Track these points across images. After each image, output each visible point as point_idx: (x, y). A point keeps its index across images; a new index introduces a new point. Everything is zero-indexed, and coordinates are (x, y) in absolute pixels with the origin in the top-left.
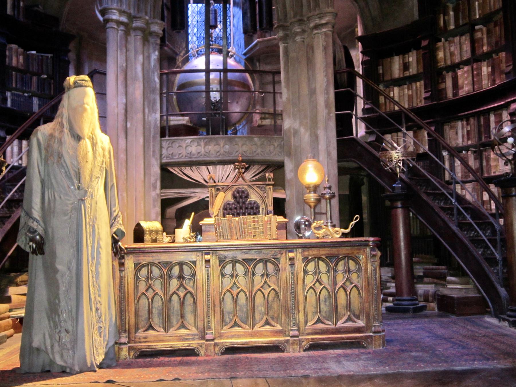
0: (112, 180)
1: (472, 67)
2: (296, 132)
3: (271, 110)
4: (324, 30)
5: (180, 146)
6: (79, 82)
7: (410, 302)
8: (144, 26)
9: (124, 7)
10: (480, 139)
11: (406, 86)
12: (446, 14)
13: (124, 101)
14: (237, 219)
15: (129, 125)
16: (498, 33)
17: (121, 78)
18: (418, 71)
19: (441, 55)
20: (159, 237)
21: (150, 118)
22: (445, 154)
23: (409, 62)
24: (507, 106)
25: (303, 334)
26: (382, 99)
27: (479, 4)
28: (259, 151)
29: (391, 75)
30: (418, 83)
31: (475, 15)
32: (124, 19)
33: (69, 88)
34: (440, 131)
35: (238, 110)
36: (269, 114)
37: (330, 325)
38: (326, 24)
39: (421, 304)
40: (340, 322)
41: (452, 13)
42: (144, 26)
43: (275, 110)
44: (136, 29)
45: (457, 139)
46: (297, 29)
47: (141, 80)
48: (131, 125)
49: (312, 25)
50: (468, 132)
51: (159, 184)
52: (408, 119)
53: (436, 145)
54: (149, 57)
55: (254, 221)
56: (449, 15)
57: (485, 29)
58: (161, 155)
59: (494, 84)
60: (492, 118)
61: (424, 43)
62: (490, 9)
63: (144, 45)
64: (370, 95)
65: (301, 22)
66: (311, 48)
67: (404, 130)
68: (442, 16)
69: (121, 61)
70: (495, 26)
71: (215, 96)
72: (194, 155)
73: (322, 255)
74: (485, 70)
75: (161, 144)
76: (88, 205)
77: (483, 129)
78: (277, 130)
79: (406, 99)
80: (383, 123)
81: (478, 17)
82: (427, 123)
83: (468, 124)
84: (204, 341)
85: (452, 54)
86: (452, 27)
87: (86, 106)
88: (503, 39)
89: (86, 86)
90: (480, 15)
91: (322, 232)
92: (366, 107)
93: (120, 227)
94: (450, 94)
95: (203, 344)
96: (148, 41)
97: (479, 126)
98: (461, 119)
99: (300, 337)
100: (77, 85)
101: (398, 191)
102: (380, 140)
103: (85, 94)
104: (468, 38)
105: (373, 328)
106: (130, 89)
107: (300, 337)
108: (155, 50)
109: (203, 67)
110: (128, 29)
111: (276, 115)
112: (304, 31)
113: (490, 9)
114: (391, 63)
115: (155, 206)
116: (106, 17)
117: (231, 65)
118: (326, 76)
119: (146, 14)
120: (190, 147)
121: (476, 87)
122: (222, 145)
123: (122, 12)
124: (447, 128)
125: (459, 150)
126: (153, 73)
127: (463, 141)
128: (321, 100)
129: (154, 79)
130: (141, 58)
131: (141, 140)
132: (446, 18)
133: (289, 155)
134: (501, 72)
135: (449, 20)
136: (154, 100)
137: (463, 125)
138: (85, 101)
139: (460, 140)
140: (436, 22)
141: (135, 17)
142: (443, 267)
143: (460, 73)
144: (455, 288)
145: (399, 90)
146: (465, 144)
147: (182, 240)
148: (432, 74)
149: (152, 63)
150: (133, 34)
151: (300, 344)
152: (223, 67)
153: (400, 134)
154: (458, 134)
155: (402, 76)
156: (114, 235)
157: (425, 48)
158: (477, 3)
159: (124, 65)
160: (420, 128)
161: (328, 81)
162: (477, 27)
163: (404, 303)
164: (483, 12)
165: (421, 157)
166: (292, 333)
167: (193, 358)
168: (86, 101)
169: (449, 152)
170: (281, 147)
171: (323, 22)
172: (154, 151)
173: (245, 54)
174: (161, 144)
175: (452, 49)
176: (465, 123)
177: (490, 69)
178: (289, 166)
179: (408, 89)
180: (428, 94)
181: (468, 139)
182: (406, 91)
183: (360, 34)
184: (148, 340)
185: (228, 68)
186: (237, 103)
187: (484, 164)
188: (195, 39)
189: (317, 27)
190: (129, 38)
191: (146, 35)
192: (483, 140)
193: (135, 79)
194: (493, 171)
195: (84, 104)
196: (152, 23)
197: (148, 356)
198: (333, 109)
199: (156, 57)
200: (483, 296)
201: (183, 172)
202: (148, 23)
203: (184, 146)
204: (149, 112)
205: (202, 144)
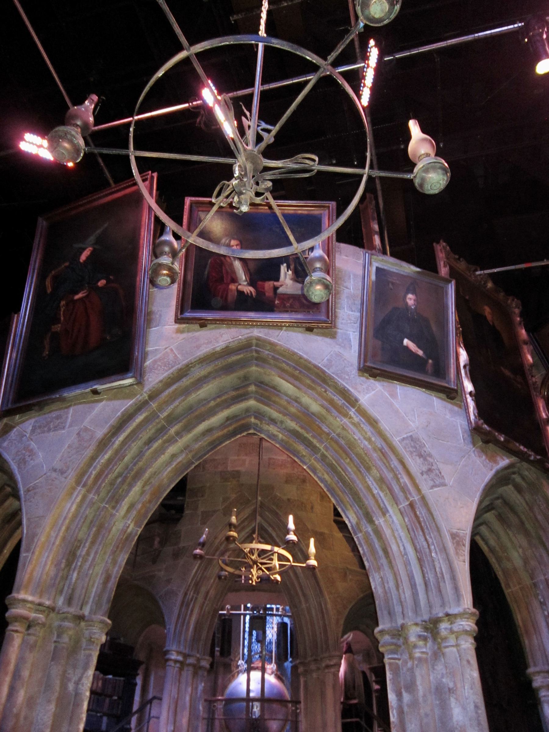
8: (195, 662)
9: (182, 649)
32: (180, 658)
42: (195, 662)
119: (198, 652)
123: (179, 653)
150: (186, 668)
190: (182, 673)
191: (197, 668)
202: (198, 660)
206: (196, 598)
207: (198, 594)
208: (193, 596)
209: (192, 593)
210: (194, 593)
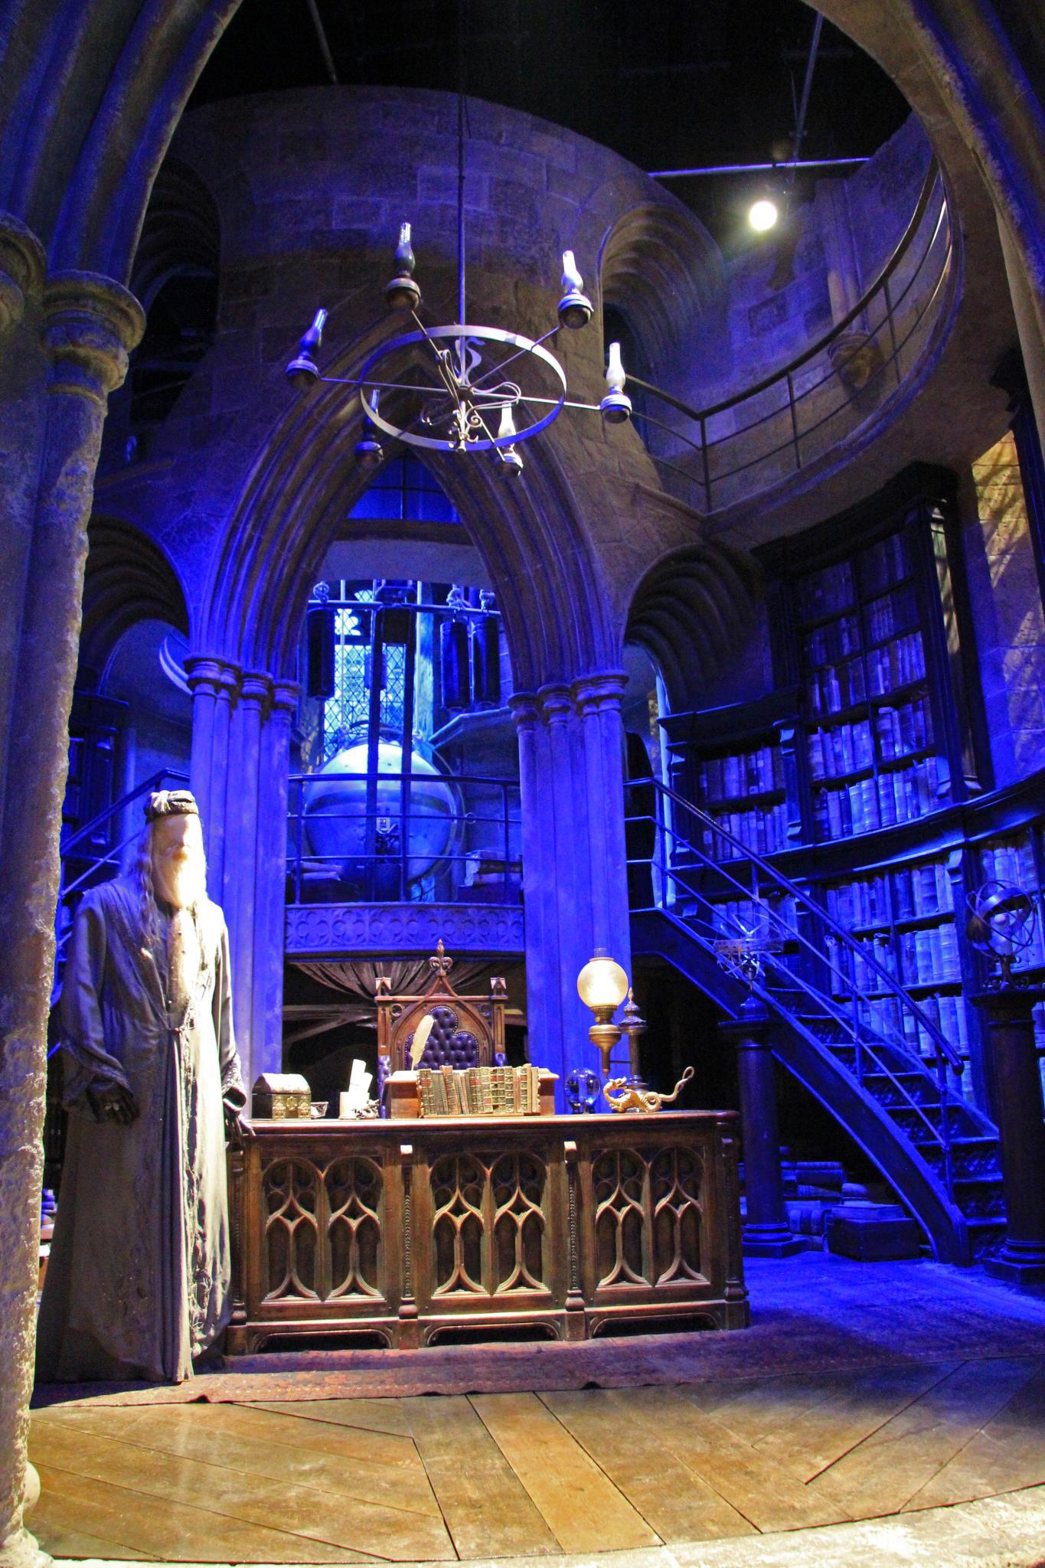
0: (224, 993)
1: (876, 783)
2: (550, 900)
3: (501, 854)
4: (603, 707)
5: (323, 922)
7: (775, 1236)
9: (230, 657)
10: (895, 916)
11: (753, 814)
12: (824, 683)
13: (221, 831)
14: (461, 1073)
15: (227, 880)
16: (921, 723)
17: (218, 788)
18: (774, 785)
19: (817, 757)
20: (303, 1106)
21: (267, 866)
22: (830, 943)
23: (757, 769)
24: (943, 856)
25: (591, 1304)
26: (708, 837)
27: (884, 669)
28: (476, 934)
29: (723, 791)
30: (776, 809)
31: (878, 688)
32: (227, 678)
34: (821, 899)
35: (425, 853)
36: (496, 862)
37: (644, 1284)
38: (609, 697)
39: (797, 1238)
40: (663, 1278)
41: (834, 683)
43: (507, 856)
44: (246, 697)
45: (852, 915)
46: (551, 704)
47: (254, 792)
48: (232, 879)
49: (581, 697)
50: (872, 902)
51: (279, 996)
52: (763, 876)
53: (814, 926)
54: (270, 748)
55: (494, 1079)
56: (829, 685)
57: (896, 714)
58: (286, 938)
59: (919, 815)
60: (916, 878)
61: (787, 735)
62: (905, 679)
63: (262, 726)
64: (685, 826)
65: (559, 691)
66: (578, 741)
67: (756, 897)
68: (817, 686)
69: (220, 754)
70: (915, 709)
71: (385, 825)
72: (349, 940)
73: (630, 1145)
74: (900, 788)
75: (286, 917)
76: (183, 1041)
77: (901, 897)
78: (514, 894)
79: (754, 837)
80: (711, 883)
81: (882, 692)
82: (797, 884)
83: (871, 888)
84: (397, 1318)
85: (838, 757)
86: (836, 708)
88: (931, 734)
89: (188, 812)
90: (886, 688)
91: (624, 1099)
92: (679, 850)
94: (835, 831)
95: (395, 1322)
96: (268, 719)
97: (894, 892)
98: (859, 877)
99: (587, 1310)
101: (748, 1018)
102: (706, 915)
103: (183, 827)
104: (867, 728)
105: (727, 1290)
106: (232, 809)
107: (587, 1310)
108: (281, 737)
109: (363, 769)
110: (235, 696)
111: (509, 865)
112: (565, 708)
113: (905, 679)
114: (722, 771)
115: (269, 1041)
116: (196, 673)
117: (418, 768)
118: (609, 792)
119: (268, 670)
120: (346, 922)
121: (884, 818)
122: (405, 920)
123: (225, 666)
124: (831, 893)
125: (860, 935)
126: (276, 778)
127: (864, 921)
128: (598, 839)
129: (277, 791)
130: (254, 751)
131: (250, 910)
132: (825, 689)
133: (537, 942)
134: (931, 794)
135: (830, 693)
136: (277, 830)
137: (862, 889)
139: (857, 919)
140: (804, 698)
141: (248, 675)
142: (836, 1164)
143: (853, 791)
144: (857, 1206)
145: (741, 820)
146: (867, 926)
147: (354, 1115)
148: (807, 792)
149: (275, 763)
150: (241, 705)
151: (587, 1324)
152: (403, 769)
153: (743, 904)
154: (853, 908)
155: (744, 794)
157: (787, 744)
158: (880, 667)
159: (224, 763)
160: (784, 892)
161: (613, 801)
162: (882, 710)
163: (765, 1237)
164: (892, 684)
165: (792, 946)
166: (569, 1301)
167: (376, 1353)
169: (839, 939)
170: (521, 925)
171: (603, 692)
172: (272, 932)
173: (434, 742)
174: (286, 917)
175: (838, 748)
176: (865, 885)
177: (909, 787)
178: (534, 965)
179: (758, 819)
180: (797, 830)
181: (874, 915)
182: (753, 823)
183: (661, 715)
184: (287, 1313)
185: (413, 772)
186: (425, 836)
187: (905, 963)
188: (336, 709)
189: (591, 701)
190: (234, 713)
192: (904, 919)
193: (243, 792)
194: (921, 976)
195: (182, 845)
196: (279, 686)
197: (284, 1347)
198: (624, 854)
199: (282, 750)
200: (916, 1221)
201: (326, 976)
202: (271, 688)
203: (331, 922)
204: (266, 854)
205: (367, 918)
206: (259, 540)
207: (264, 529)
208: (251, 538)
209: (249, 526)
210: (254, 527)
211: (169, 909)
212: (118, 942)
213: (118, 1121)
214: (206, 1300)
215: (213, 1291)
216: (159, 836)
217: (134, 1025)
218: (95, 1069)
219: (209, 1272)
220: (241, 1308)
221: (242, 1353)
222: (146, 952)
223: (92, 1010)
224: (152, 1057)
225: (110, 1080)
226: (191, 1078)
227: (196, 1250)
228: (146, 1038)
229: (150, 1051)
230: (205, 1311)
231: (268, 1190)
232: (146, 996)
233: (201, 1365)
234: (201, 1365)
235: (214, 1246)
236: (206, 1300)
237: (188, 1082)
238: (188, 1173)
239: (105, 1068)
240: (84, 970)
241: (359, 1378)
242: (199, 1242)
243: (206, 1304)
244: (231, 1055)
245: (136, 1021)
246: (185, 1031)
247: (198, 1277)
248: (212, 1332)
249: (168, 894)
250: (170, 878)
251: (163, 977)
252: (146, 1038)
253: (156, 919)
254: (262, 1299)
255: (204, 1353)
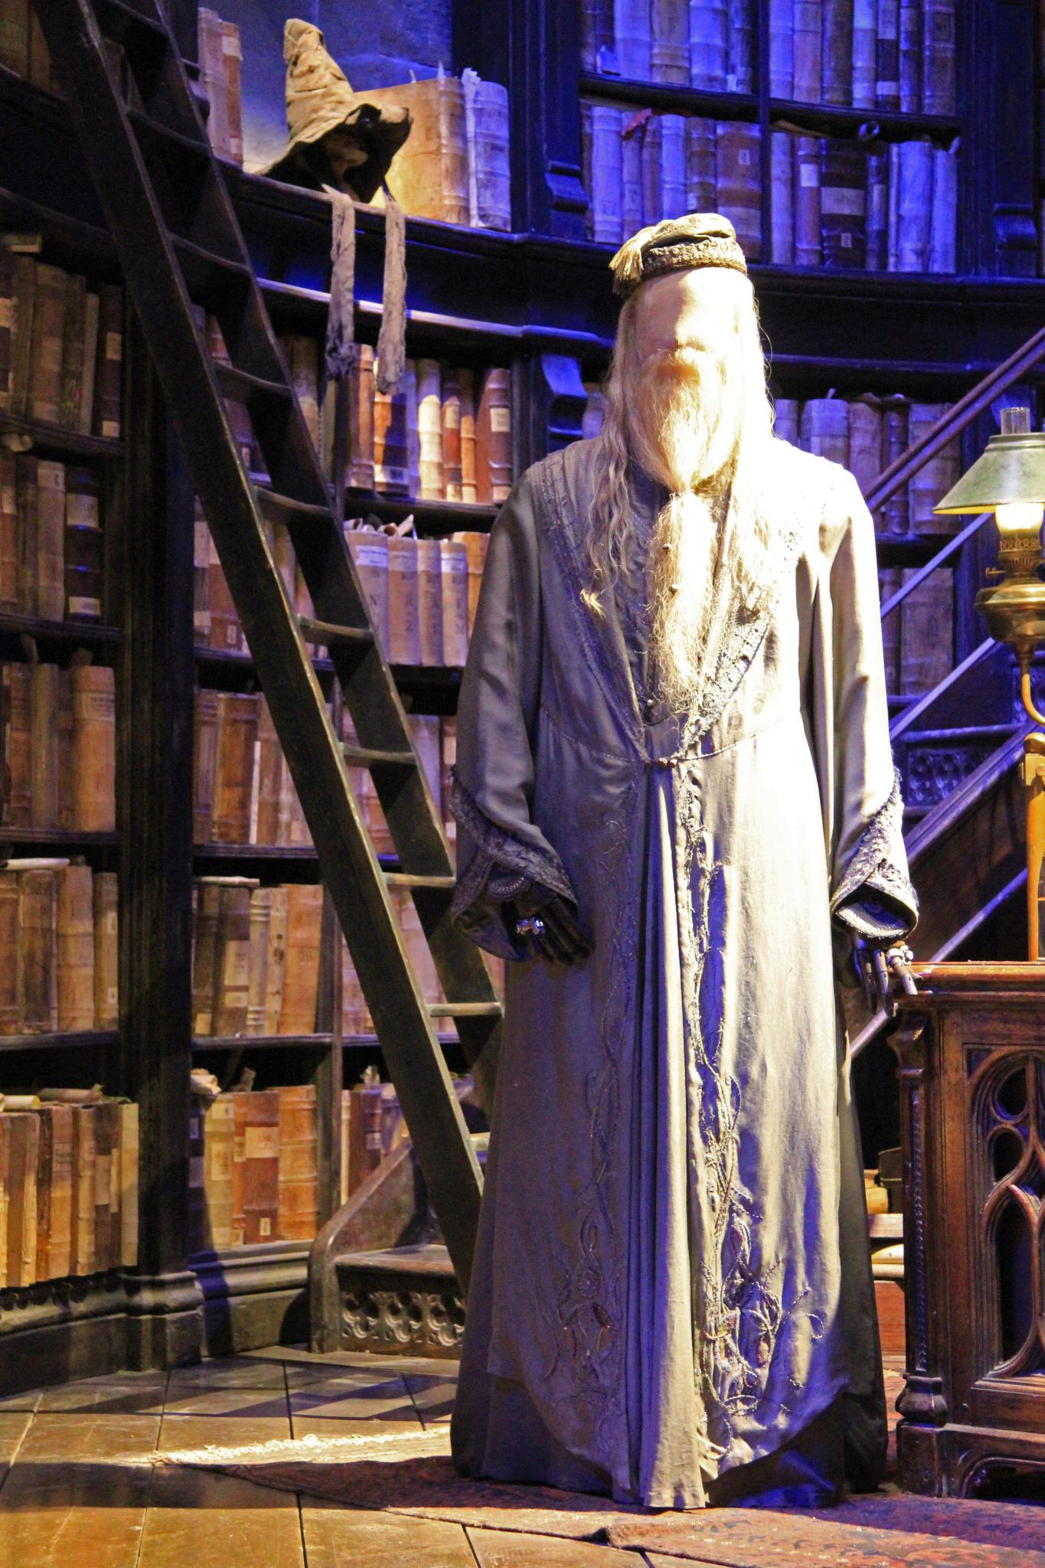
6: (656, 251)
33: (631, 288)
76: (683, 787)
87: (686, 356)
89: (688, 266)
93: (878, 880)
100: (658, 266)
103: (678, 303)
138: (682, 336)
156: (849, 915)
168: (684, 331)
195: (674, 346)
211: (655, 494)
212: (557, 578)
213: (550, 959)
214: (766, 1352)
215: (785, 1331)
216: (638, 326)
217: (578, 755)
218: (492, 851)
219: (775, 1289)
220: (935, 1389)
221: (926, 1490)
222: (591, 600)
223: (504, 729)
224: (612, 823)
225: (515, 873)
226: (708, 864)
227: (732, 1238)
228: (599, 783)
229: (604, 811)
230: (764, 1373)
231: (987, 1122)
232: (600, 691)
233: (732, 1488)
234: (732, 1488)
235: (786, 1234)
236: (766, 1352)
237: (696, 873)
238: (702, 1069)
239: (511, 848)
240: (494, 646)
241: (877, 1542)
242: (742, 1222)
243: (767, 1357)
244: (869, 809)
245: (583, 750)
246: (692, 764)
247: (742, 1295)
248: (782, 1421)
249: (651, 462)
250: (653, 429)
251: (633, 643)
252: (599, 783)
253: (625, 517)
254: (980, 1373)
255: (758, 1462)
